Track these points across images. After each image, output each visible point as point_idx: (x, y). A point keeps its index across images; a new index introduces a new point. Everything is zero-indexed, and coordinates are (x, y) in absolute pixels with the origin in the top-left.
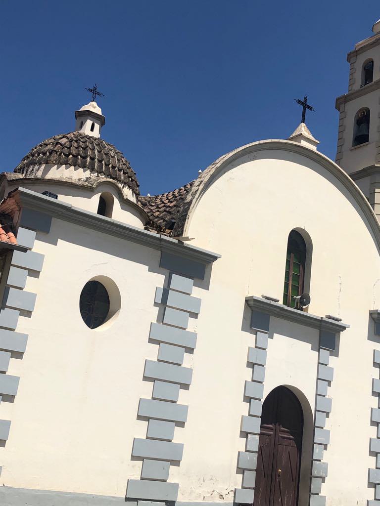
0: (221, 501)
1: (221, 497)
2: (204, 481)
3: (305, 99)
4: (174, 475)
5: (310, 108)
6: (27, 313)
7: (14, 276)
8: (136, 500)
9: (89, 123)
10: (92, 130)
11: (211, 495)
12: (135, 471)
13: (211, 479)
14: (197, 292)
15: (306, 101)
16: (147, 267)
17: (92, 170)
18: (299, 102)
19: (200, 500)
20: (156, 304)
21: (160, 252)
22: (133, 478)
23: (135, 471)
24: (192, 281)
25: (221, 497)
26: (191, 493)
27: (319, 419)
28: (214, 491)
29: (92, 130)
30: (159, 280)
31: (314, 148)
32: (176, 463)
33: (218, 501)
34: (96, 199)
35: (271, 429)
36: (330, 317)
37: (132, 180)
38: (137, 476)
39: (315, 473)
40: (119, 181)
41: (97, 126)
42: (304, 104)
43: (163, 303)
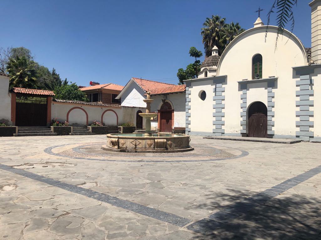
1: (237, 132)
4: (223, 127)
5: (261, 10)
6: (190, 102)
7: (187, 96)
8: (215, 133)
9: (213, 52)
12: (214, 127)
14: (223, 86)
16: (211, 85)
17: (205, 67)
19: (231, 133)
20: (214, 92)
21: (213, 80)
23: (214, 127)
24: (221, 84)
25: (237, 132)
27: (268, 109)
30: (214, 87)
31: (260, 25)
32: (224, 125)
34: (204, 73)
35: (257, 114)
36: (269, 77)
37: (216, 63)
38: (215, 128)
39: (268, 123)
40: (210, 66)
41: (214, 52)
43: (215, 91)
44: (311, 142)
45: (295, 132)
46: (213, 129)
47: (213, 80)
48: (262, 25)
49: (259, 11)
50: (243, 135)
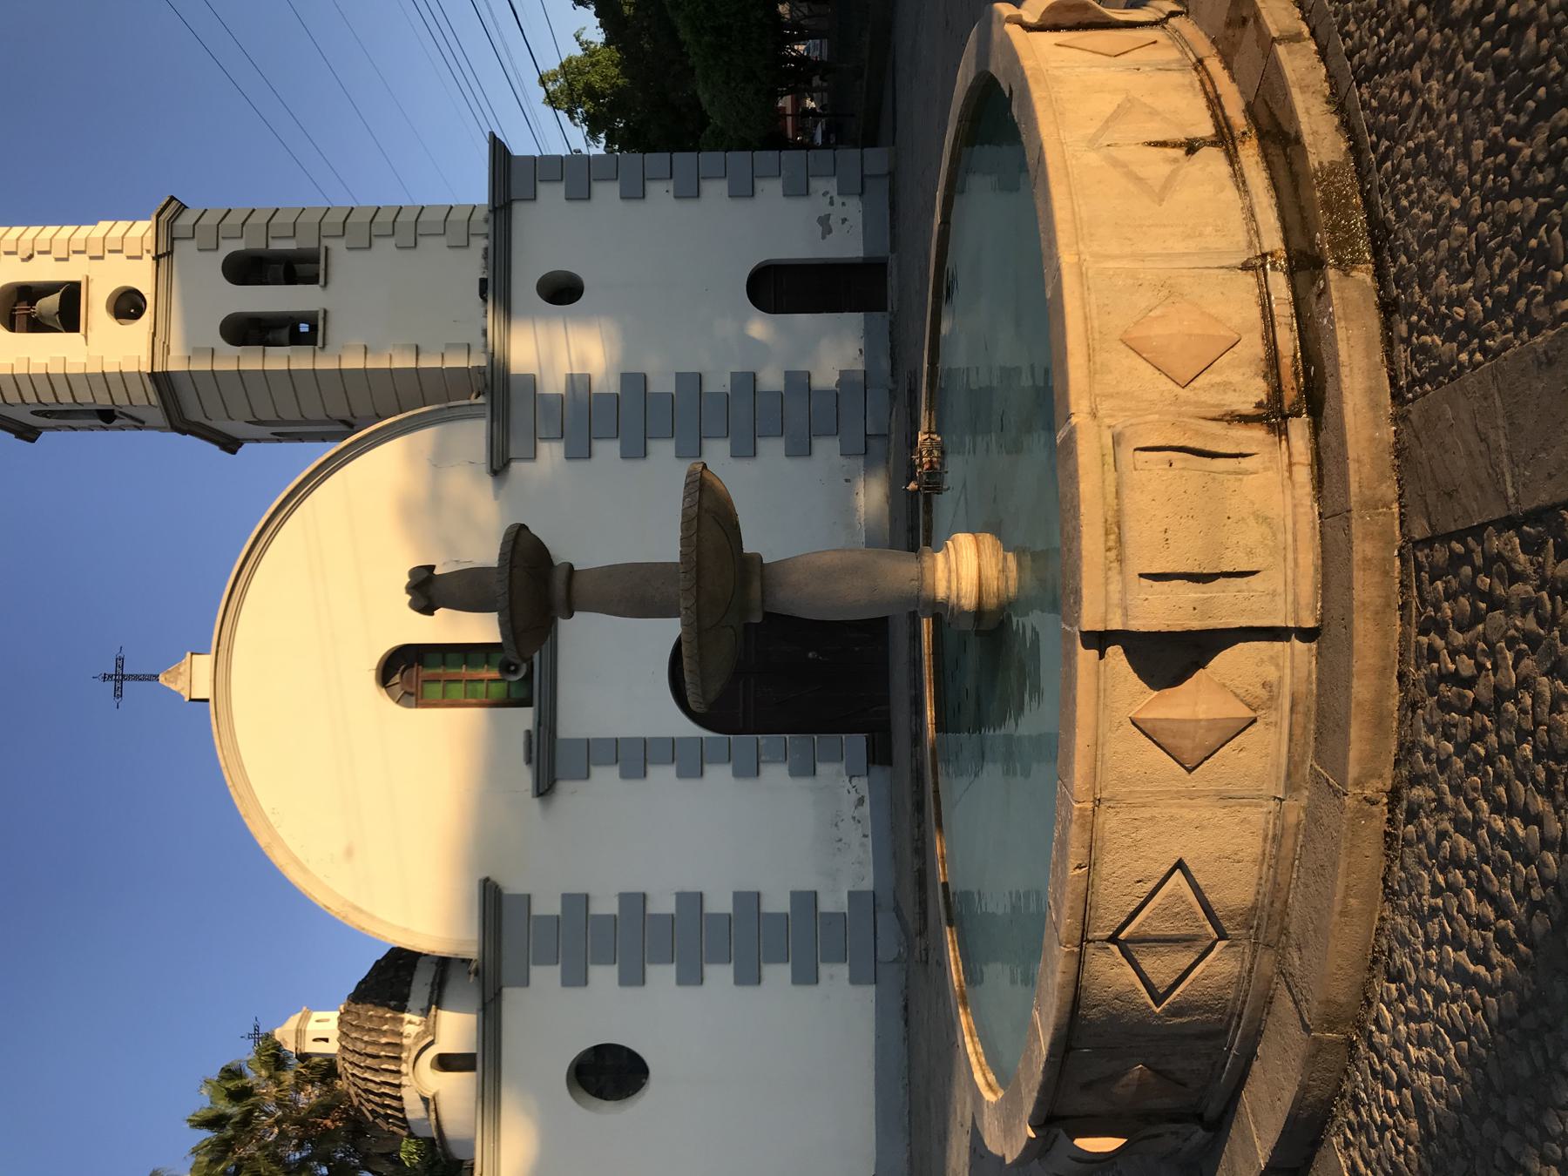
0: (867, 801)
2: (840, 840)
3: (106, 678)
10: (326, 1040)
11: (859, 822)
13: (836, 825)
15: (110, 676)
18: (118, 692)
19: (869, 841)
22: (847, 976)
25: (861, 801)
26: (859, 863)
28: (854, 818)
29: (326, 1040)
33: (866, 808)
42: (119, 678)
44: (895, 382)
45: (844, 461)
46: (855, 980)
47: (505, 990)
48: (208, 653)
49: (119, 678)
50: (879, 755)
